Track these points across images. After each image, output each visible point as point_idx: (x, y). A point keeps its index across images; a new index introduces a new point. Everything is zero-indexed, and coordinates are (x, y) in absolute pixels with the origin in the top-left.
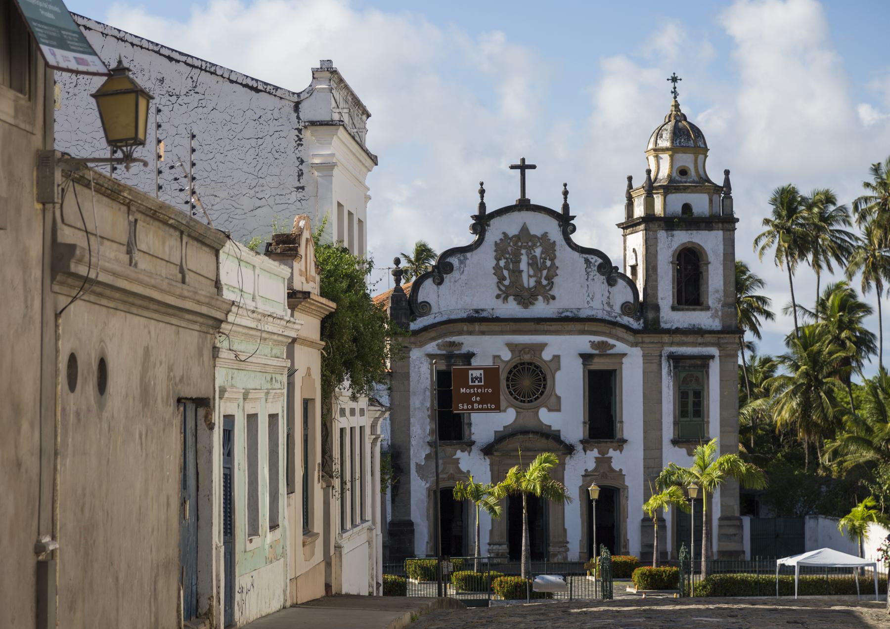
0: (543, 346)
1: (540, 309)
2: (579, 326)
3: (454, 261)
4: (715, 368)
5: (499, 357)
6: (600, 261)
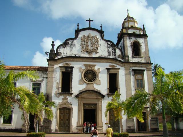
0: (95, 66)
1: (94, 55)
2: (106, 61)
3: (70, 42)
4: (145, 73)
5: (81, 68)
6: (111, 44)
